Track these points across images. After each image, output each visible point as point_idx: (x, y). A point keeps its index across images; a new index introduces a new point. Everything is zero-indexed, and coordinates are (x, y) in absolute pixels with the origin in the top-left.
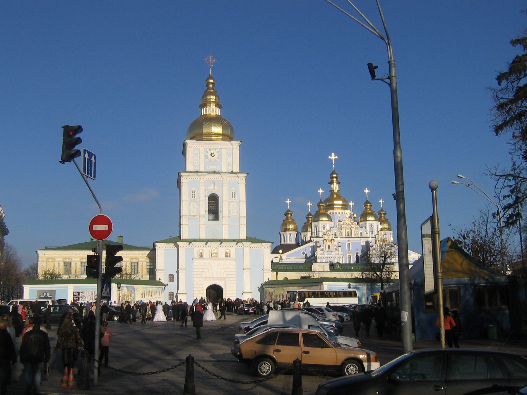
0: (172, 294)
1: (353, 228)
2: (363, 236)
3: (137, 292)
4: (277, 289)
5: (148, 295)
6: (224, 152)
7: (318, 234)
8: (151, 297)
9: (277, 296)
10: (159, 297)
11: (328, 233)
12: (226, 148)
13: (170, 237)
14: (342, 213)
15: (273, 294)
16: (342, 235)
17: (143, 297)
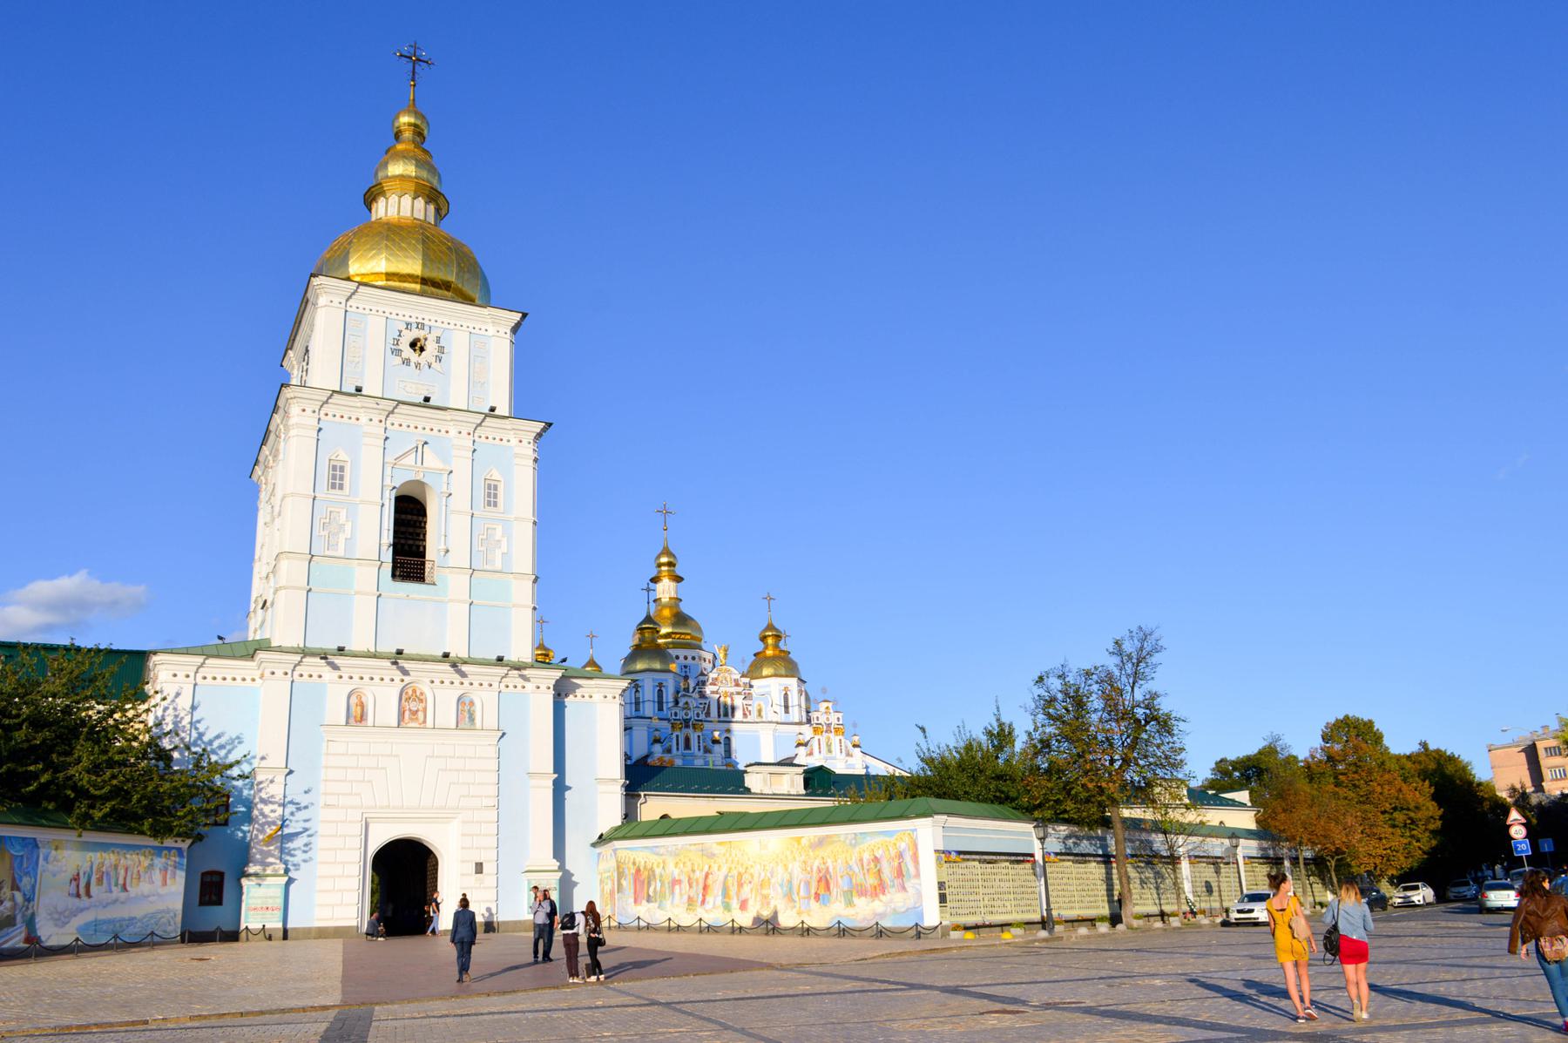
0: (216, 878)
1: (738, 693)
2: (764, 720)
3: (50, 867)
4: (677, 855)
5: (109, 884)
6: (458, 345)
7: (641, 709)
8: (123, 895)
9: (675, 882)
10: (162, 891)
11: (687, 703)
12: (471, 330)
13: (220, 638)
14: (694, 658)
15: (653, 871)
16: (708, 714)
17: (82, 891)
